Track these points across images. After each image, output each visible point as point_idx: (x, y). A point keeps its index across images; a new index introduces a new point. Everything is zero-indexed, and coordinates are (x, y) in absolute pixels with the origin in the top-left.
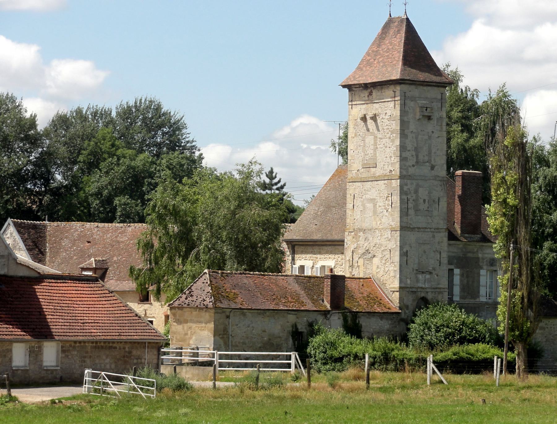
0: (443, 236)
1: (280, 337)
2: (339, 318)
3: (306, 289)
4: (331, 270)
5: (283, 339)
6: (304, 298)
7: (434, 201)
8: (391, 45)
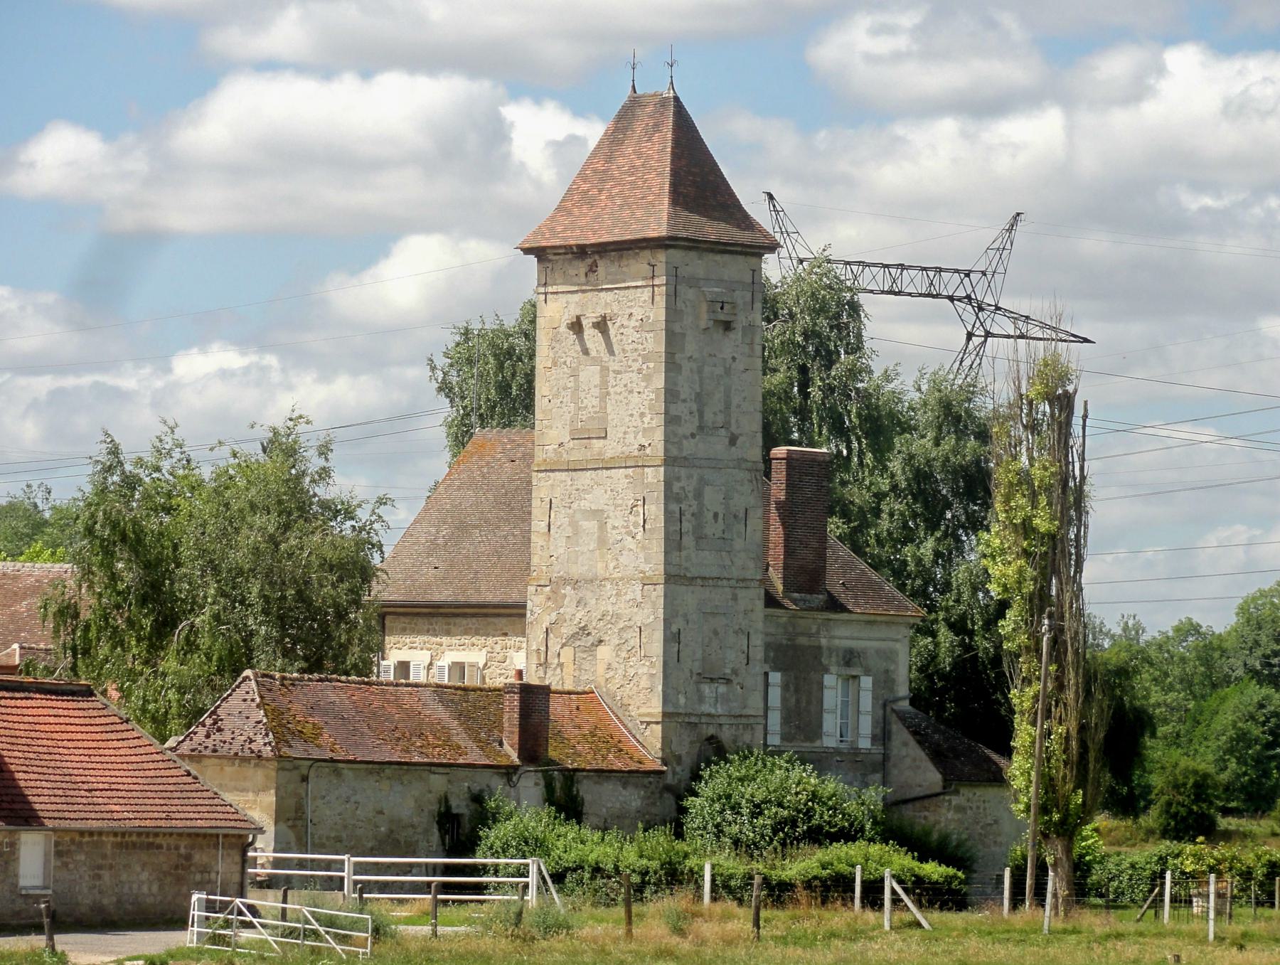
0: (753, 599)
1: (413, 826)
2: (537, 784)
3: (463, 717)
4: (520, 674)
5: (419, 830)
6: (460, 737)
7: (735, 516)
8: (639, 158)
